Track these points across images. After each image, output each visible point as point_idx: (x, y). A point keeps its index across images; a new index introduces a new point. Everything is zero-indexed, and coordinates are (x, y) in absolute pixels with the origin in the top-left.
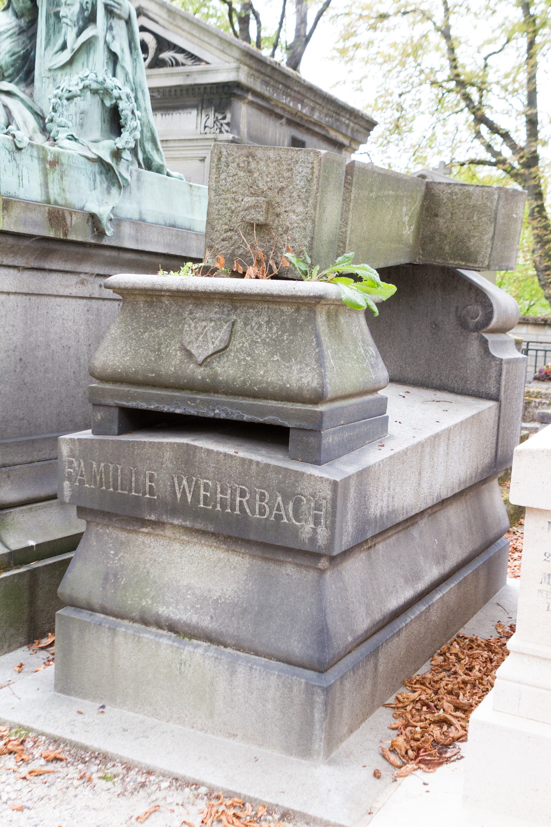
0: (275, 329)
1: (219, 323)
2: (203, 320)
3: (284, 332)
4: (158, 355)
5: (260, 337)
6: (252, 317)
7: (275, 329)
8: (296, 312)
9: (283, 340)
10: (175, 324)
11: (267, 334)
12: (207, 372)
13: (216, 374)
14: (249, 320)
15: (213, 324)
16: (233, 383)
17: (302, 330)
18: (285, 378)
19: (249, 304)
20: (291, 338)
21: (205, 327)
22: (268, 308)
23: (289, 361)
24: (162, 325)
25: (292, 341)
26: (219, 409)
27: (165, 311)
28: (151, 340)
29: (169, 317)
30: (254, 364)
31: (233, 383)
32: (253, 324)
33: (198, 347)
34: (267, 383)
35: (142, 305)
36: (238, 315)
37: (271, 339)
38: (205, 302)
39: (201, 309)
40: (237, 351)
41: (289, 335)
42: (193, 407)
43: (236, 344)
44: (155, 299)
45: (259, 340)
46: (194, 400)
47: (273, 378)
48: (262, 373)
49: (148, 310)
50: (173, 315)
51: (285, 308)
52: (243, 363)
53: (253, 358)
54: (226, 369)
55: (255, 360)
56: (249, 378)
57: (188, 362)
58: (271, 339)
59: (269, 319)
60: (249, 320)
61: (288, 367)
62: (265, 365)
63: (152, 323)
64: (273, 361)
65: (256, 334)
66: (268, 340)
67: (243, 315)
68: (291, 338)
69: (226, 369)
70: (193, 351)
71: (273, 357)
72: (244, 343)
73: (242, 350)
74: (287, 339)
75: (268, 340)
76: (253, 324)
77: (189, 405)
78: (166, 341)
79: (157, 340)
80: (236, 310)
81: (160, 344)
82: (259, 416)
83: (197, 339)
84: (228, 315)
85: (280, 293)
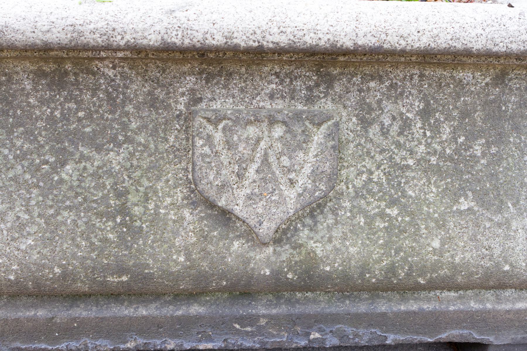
0: (446, 131)
1: (298, 129)
2: (249, 123)
3: (472, 137)
4: (123, 224)
5: (412, 152)
6: (379, 102)
7: (446, 131)
8: (496, 85)
9: (473, 156)
10: (154, 133)
11: (428, 145)
12: (284, 257)
13: (311, 255)
14: (371, 109)
15: (278, 131)
16: (362, 274)
17: (516, 128)
18: (497, 252)
19: (367, 70)
20: (494, 150)
21: (258, 141)
22: (421, 76)
23: (499, 210)
24: (114, 140)
25: (497, 159)
26: (320, 330)
27: (111, 99)
28: (89, 183)
29: (127, 114)
30: (410, 223)
31: (362, 274)
32: (387, 122)
33: (249, 197)
34: (454, 267)
35: (28, 86)
36: (339, 99)
37: (442, 156)
38: (232, 68)
39: (225, 87)
40: (357, 195)
41: (488, 144)
42: (252, 335)
43: (353, 177)
44: (68, 66)
45: (411, 162)
46: (252, 320)
47: (468, 255)
48: (436, 244)
49: (52, 99)
50: (137, 108)
51: (465, 75)
52: (380, 224)
53: (404, 210)
54: (337, 243)
55: (411, 214)
56: (405, 260)
57: (222, 237)
58: (442, 156)
59: (428, 104)
60: (371, 109)
61: (499, 225)
62: (441, 224)
63: (77, 137)
64: (460, 213)
65: (399, 145)
66: (434, 160)
67: (353, 98)
68: (494, 150)
69: (337, 243)
70: (238, 210)
71: (456, 201)
72: (371, 173)
73: (369, 192)
74: (484, 155)
75: (434, 160)
76: (387, 122)
77: (238, 332)
78: (138, 182)
79: (108, 183)
80: (330, 86)
81: (122, 194)
82: (425, 334)
83: (240, 176)
84: (310, 100)
85: (490, 46)
